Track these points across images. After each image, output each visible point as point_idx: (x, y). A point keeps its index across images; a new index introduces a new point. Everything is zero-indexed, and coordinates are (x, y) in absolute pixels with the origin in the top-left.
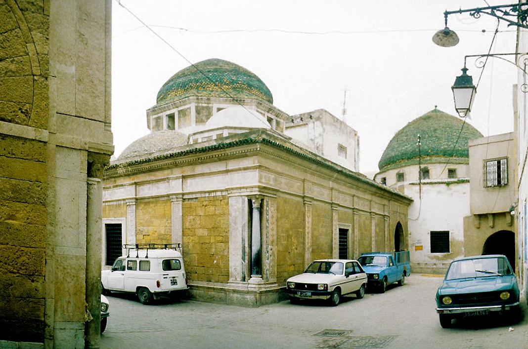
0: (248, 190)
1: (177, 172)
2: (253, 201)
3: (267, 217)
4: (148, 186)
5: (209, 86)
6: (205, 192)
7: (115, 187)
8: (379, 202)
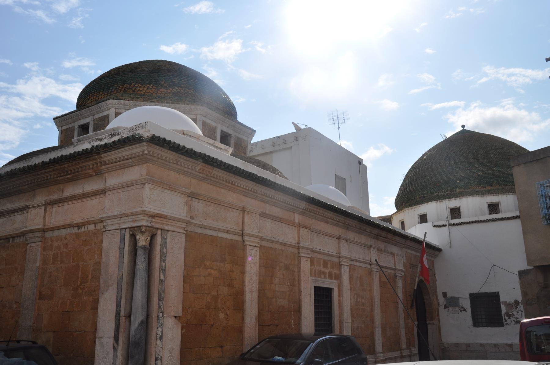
0: (131, 218)
1: (41, 198)
2: (138, 237)
3: (164, 264)
5: (141, 89)
6: (72, 226)
8: (363, 242)
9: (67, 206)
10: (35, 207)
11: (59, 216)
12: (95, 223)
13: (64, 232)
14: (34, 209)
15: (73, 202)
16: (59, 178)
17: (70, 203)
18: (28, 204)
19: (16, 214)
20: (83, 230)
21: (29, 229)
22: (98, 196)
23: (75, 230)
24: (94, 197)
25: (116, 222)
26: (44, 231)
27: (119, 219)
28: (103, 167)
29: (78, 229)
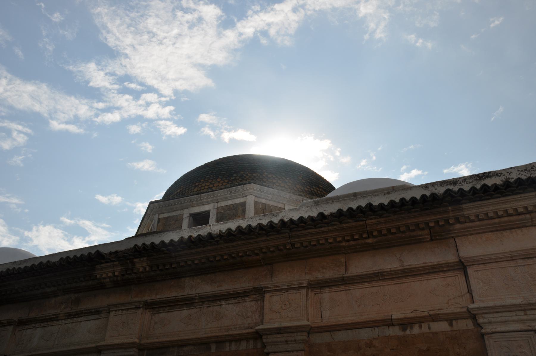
4: (185, 312)
5: (274, 181)
6: (389, 323)
7: (69, 316)
9: (357, 291)
10: (280, 290)
11: (340, 307)
12: (451, 319)
13: (365, 334)
14: (278, 293)
15: (376, 284)
16: (344, 244)
17: (367, 285)
18: (264, 283)
19: (223, 302)
20: (416, 330)
21: (276, 325)
22: (442, 275)
23: (395, 331)
24: (431, 276)
25: (515, 318)
26: (310, 330)
27: (522, 313)
28: (458, 226)
29: (404, 330)
